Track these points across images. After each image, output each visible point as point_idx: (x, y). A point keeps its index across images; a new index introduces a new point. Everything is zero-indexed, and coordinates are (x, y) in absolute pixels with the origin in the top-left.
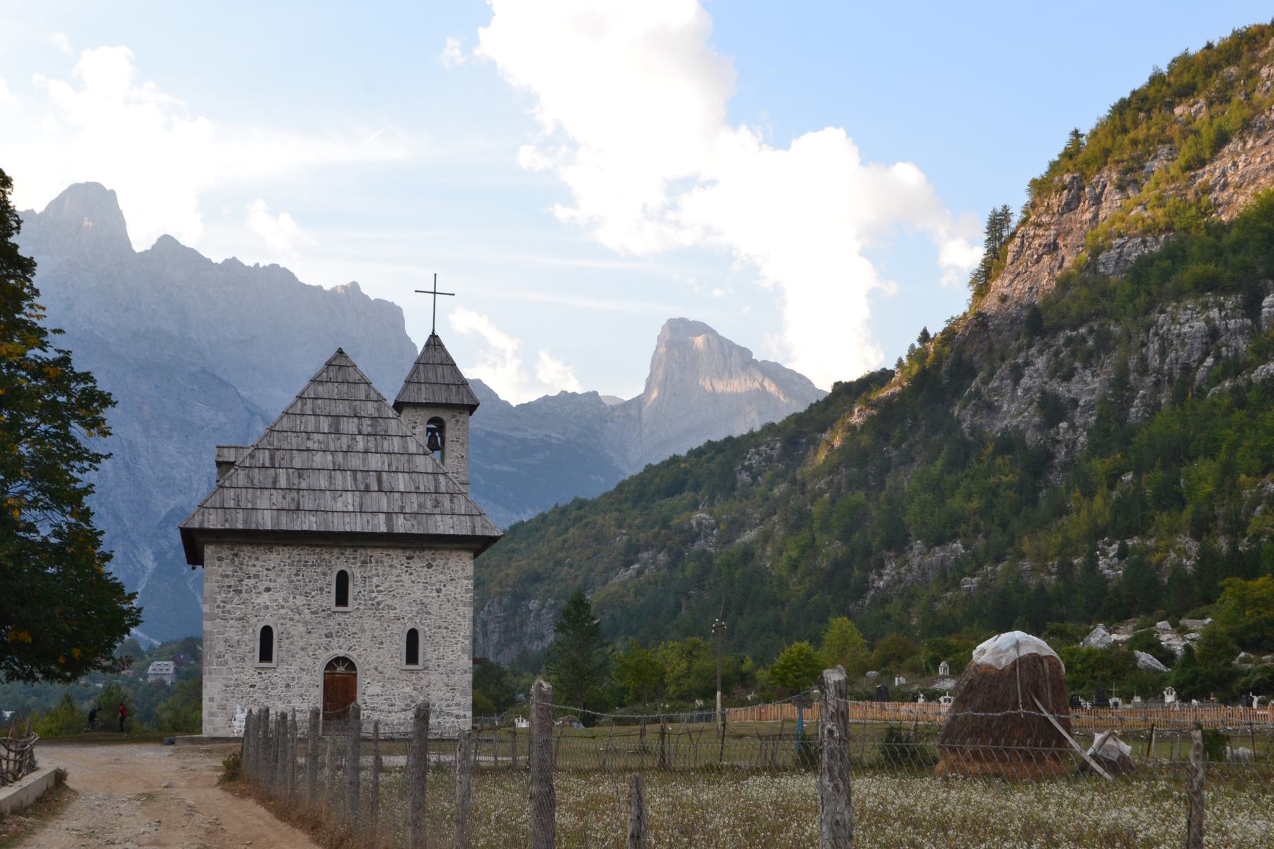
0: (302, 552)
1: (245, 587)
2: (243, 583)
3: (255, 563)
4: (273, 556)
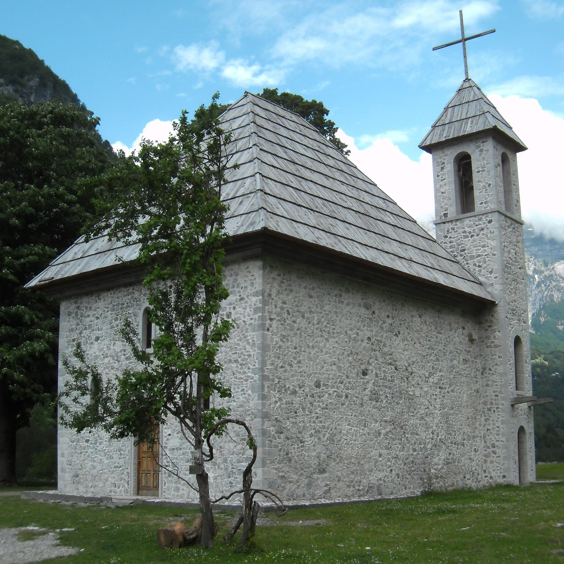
0: (120, 295)
1: (83, 339)
2: (82, 335)
3: (89, 313)
4: (101, 304)
